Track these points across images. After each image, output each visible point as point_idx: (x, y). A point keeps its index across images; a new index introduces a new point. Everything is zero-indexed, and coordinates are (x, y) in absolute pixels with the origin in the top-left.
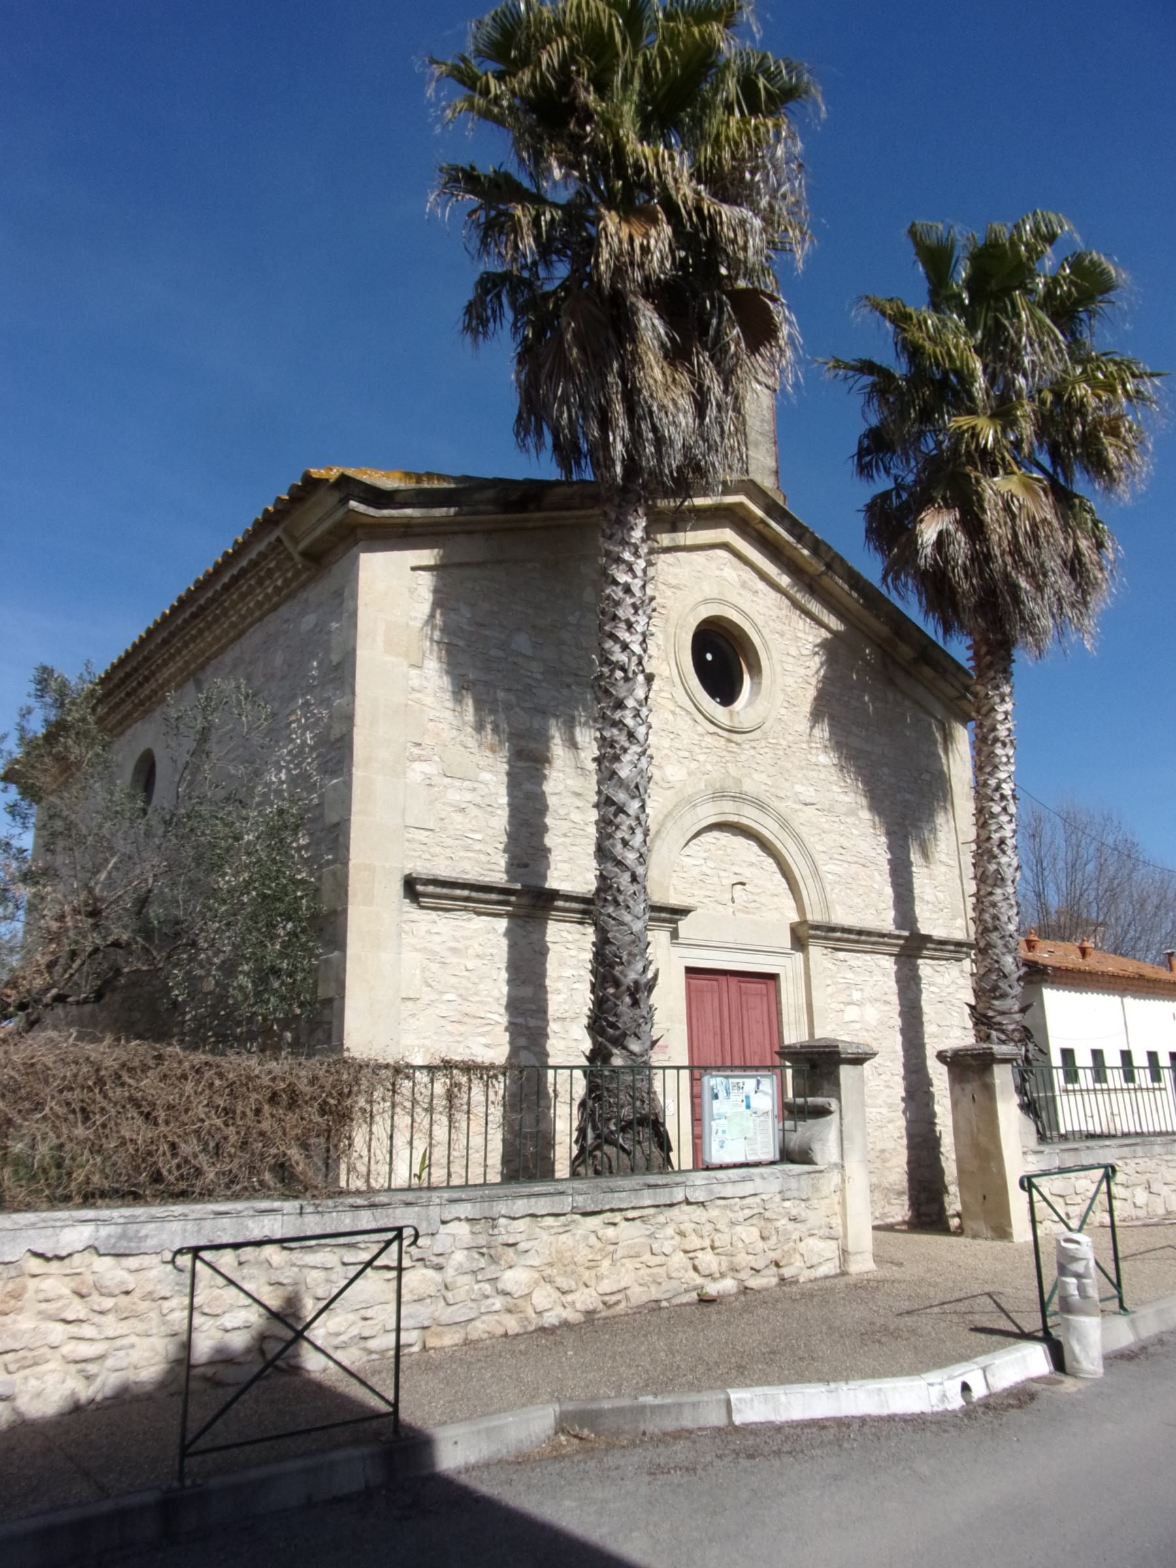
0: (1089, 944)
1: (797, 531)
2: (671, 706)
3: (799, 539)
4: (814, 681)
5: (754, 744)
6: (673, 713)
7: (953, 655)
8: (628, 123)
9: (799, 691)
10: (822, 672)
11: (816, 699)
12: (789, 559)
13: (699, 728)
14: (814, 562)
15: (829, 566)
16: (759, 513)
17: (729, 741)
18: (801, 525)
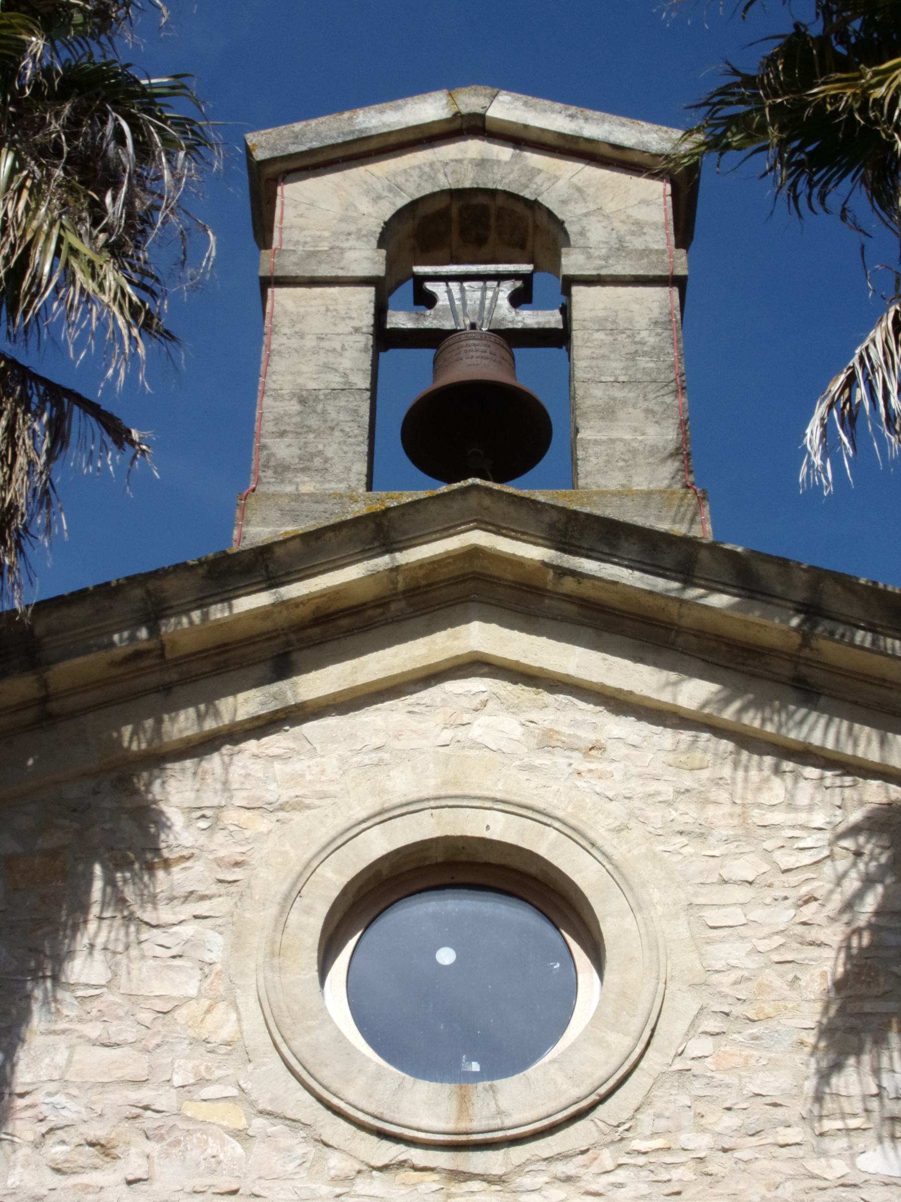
0: (867, 849)
1: (667, 561)
2: (237, 1118)
3: (686, 573)
4: (834, 935)
5: (561, 1168)
6: (242, 1136)
7: (593, 562)
8: (58, 269)
9: (771, 976)
10: (870, 903)
11: (839, 985)
12: (699, 633)
13: (336, 1163)
14: (755, 616)
15: (812, 611)
16: (534, 553)
17: (458, 1176)
18: (668, 539)
